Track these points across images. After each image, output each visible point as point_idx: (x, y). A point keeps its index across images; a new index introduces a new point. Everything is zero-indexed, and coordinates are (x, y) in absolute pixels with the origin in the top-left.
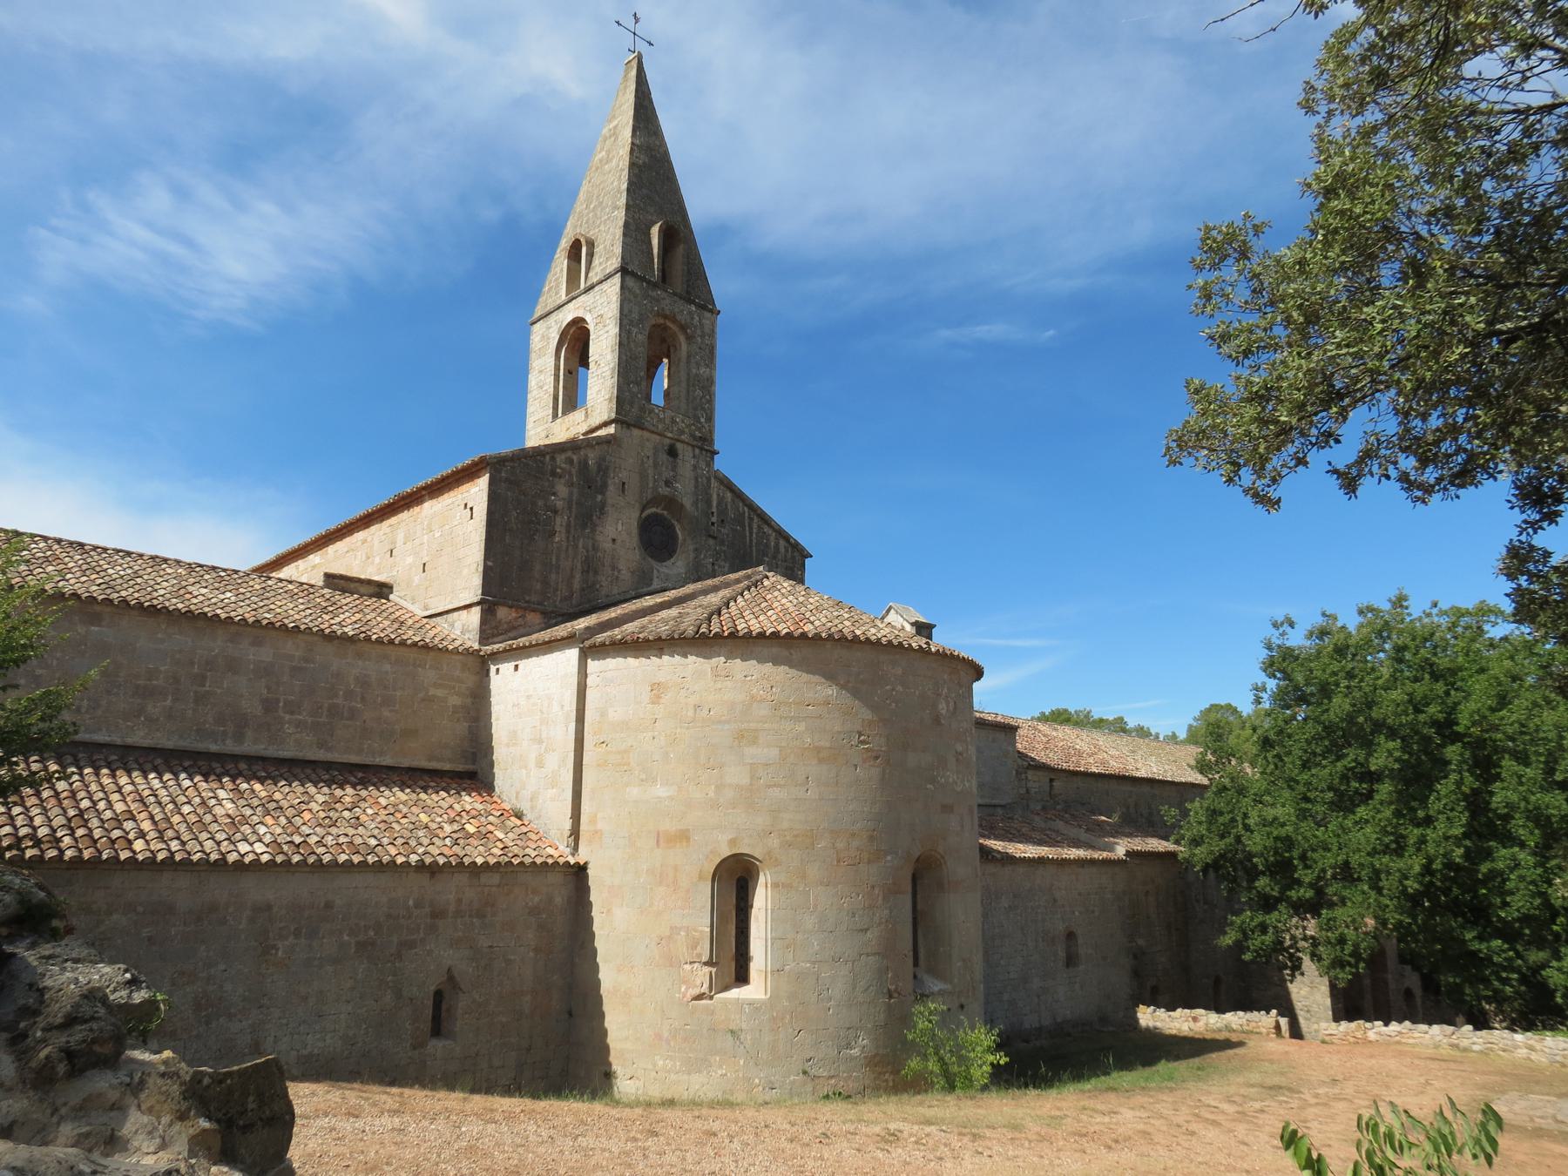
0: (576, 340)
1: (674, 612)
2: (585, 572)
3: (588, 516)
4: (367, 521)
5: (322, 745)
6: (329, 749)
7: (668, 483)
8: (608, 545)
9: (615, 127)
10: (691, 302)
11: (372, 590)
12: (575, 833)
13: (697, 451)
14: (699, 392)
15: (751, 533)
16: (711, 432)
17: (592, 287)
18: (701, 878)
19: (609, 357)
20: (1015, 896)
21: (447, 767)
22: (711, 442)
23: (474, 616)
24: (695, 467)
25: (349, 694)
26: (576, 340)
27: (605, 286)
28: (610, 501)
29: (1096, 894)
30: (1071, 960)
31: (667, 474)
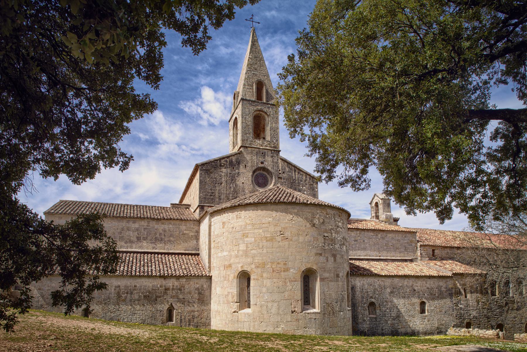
7: (262, 163)
8: (241, 185)
13: (273, 151)
15: (295, 175)
16: (278, 144)
18: (234, 278)
20: (394, 288)
25: (160, 234)
29: (437, 288)
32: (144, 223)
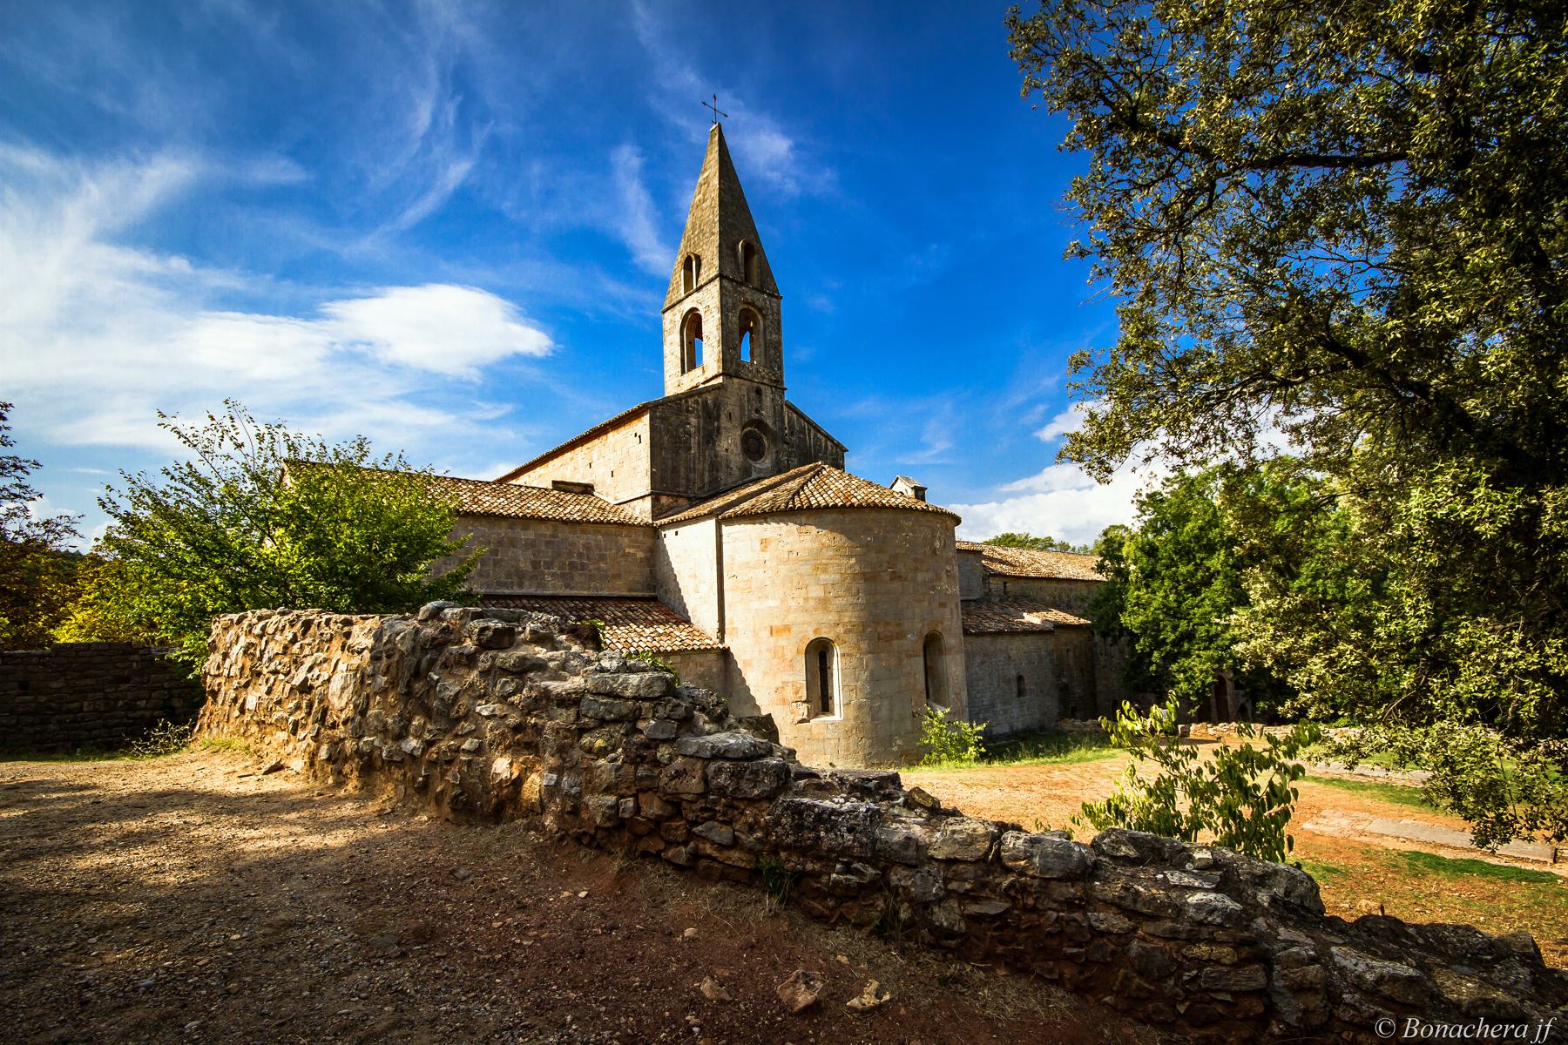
0: (692, 323)
1: (770, 494)
2: (711, 471)
3: (710, 436)
4: (572, 446)
5: (567, 586)
6: (572, 588)
7: (757, 411)
8: (724, 453)
10: (764, 292)
11: (581, 489)
12: (722, 630)
14: (772, 352)
16: (781, 376)
17: (701, 287)
18: (798, 652)
21: (640, 594)
22: (782, 383)
23: (648, 503)
24: (773, 400)
25: (580, 555)
26: (692, 323)
27: (709, 287)
30: (1021, 693)
31: (755, 404)
32: (545, 530)
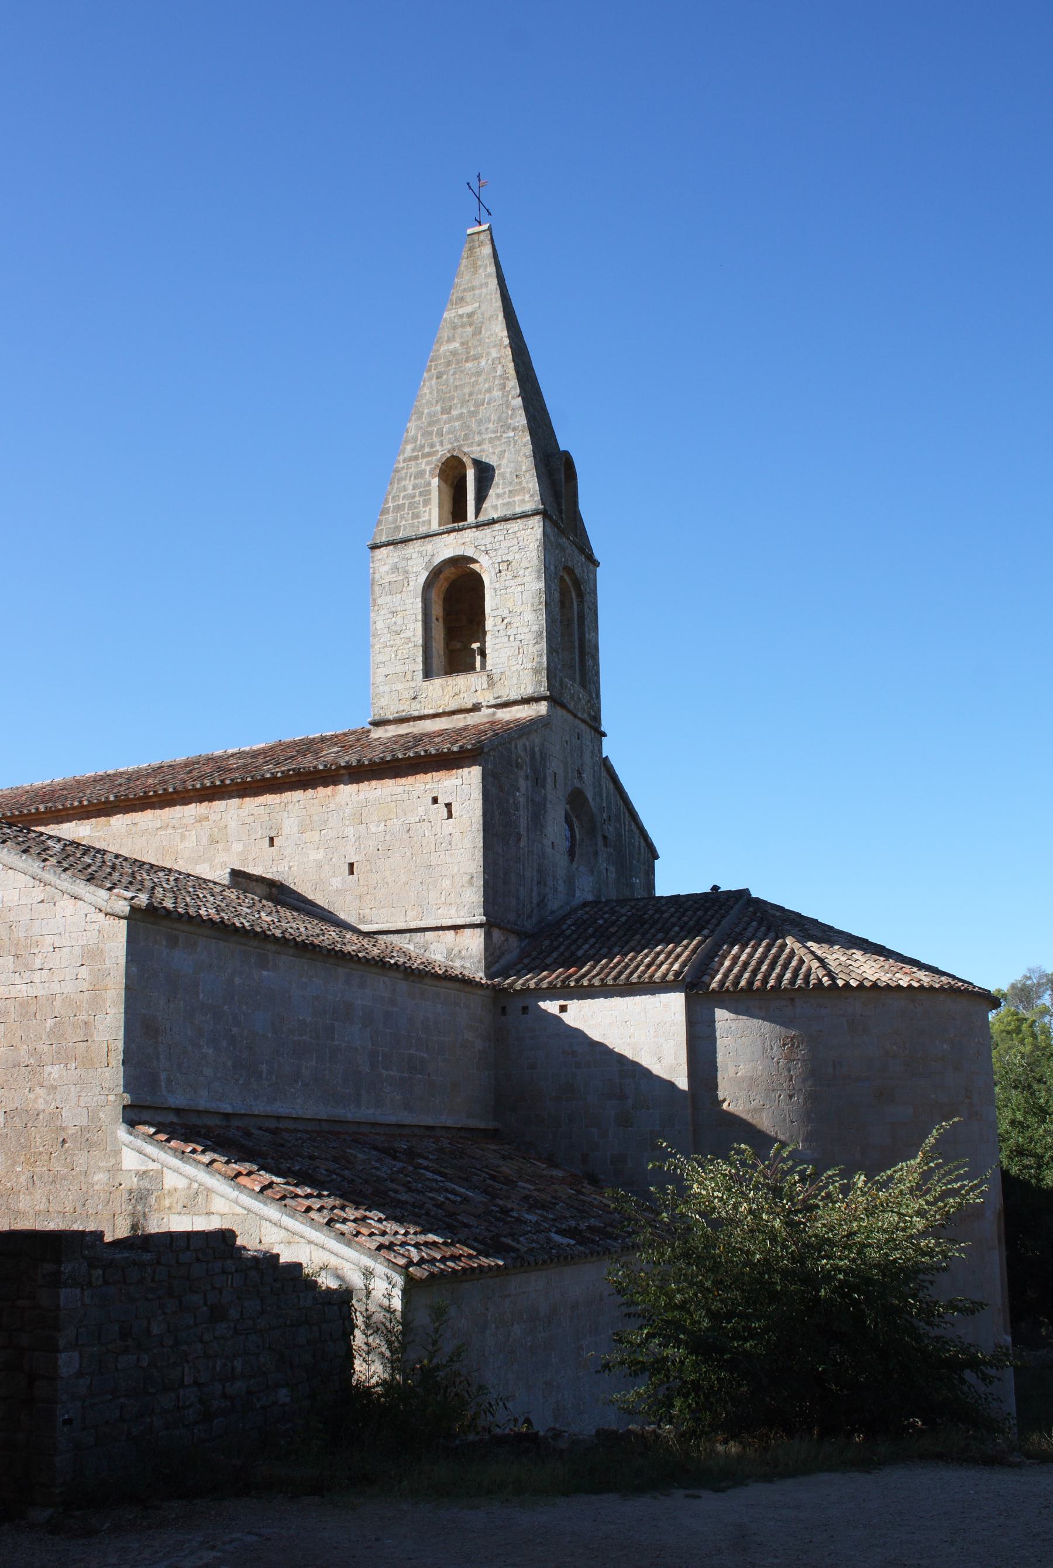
8: (549, 850)
9: (470, 315)
19: (529, 616)
28: (549, 797)
